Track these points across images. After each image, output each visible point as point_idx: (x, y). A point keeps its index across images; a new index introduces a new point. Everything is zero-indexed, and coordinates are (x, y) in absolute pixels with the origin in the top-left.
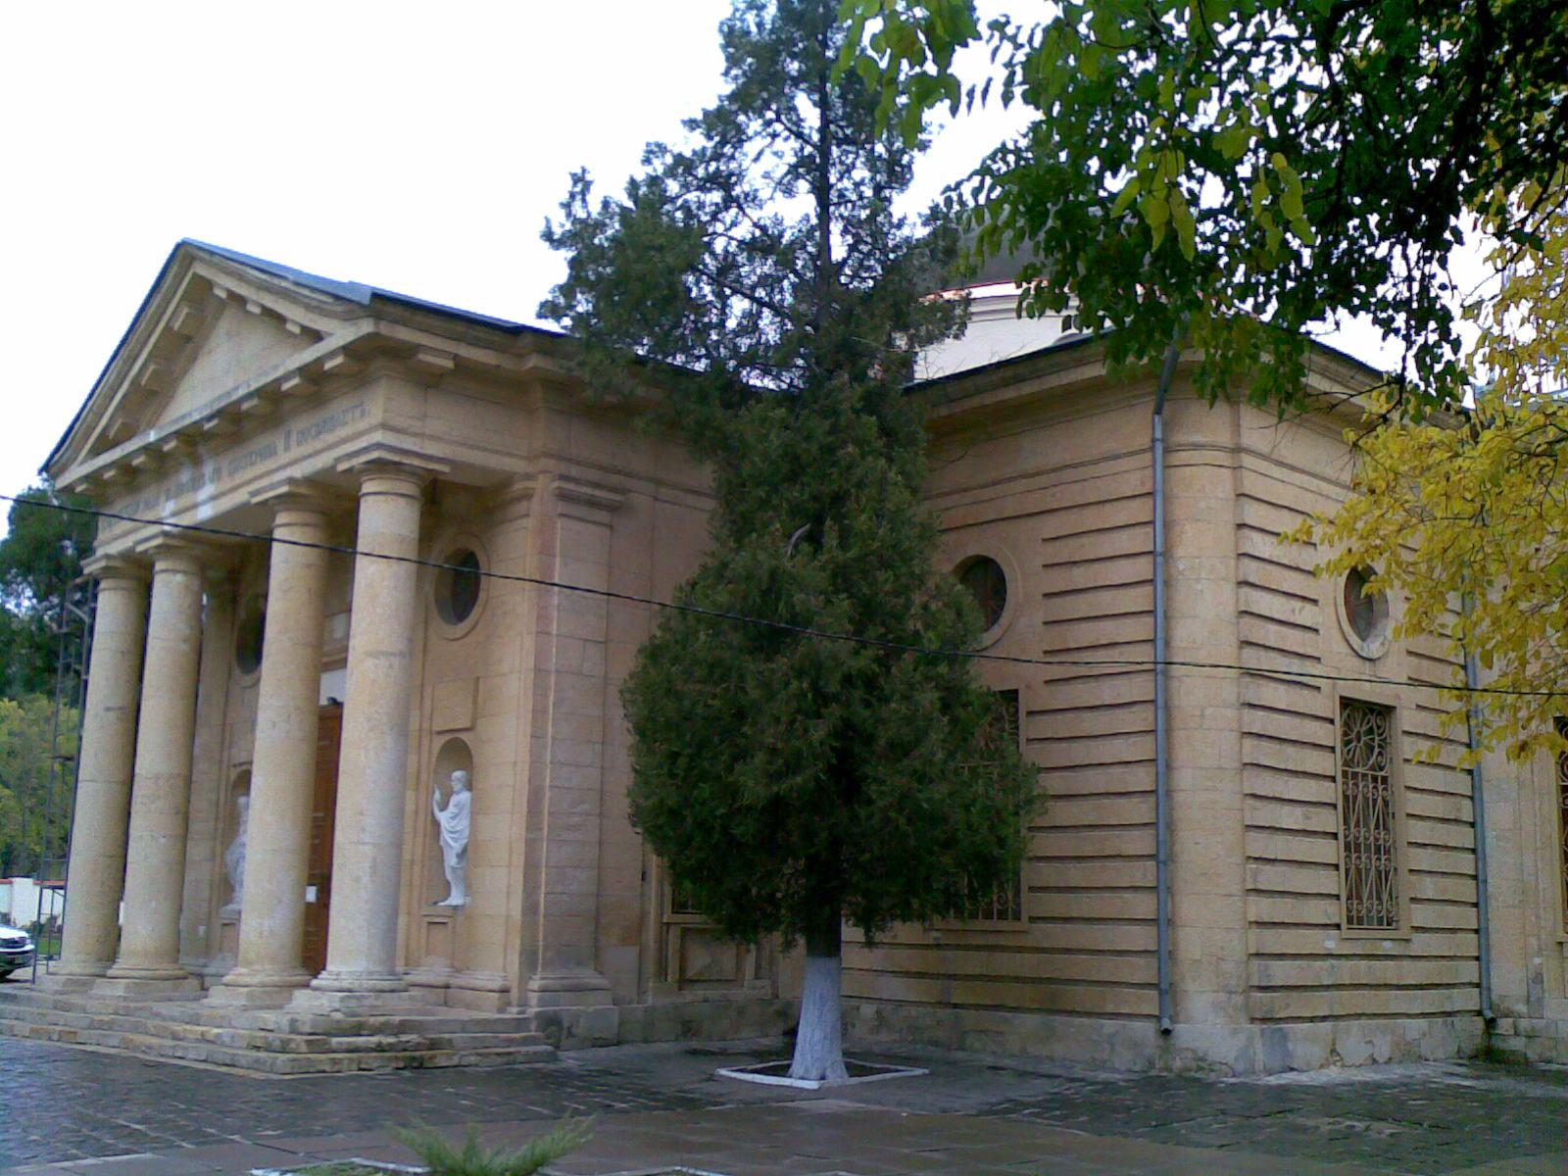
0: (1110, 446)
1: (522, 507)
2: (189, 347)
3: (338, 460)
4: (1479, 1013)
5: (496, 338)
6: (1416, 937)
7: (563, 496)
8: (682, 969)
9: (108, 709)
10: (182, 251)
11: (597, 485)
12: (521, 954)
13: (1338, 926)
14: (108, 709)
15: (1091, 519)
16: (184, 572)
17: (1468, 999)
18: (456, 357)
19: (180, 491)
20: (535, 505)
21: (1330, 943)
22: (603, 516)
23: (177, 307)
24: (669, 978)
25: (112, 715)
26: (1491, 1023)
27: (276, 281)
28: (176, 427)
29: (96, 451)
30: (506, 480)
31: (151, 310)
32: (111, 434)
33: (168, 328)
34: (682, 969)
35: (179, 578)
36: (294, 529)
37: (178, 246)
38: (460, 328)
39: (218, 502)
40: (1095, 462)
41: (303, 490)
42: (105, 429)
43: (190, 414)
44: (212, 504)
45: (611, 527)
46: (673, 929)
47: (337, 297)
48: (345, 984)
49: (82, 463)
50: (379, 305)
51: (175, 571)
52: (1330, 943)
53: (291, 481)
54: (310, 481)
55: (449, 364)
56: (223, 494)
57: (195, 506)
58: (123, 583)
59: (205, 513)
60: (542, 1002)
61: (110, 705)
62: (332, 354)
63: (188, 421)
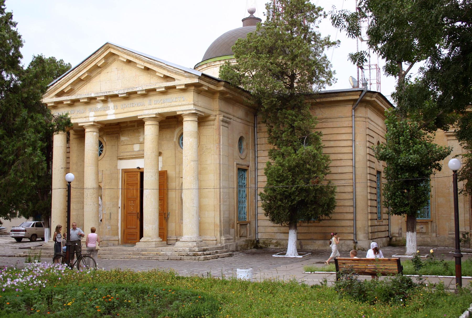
0: (340, 115)
1: (212, 123)
2: (99, 70)
3: (179, 111)
4: (388, 237)
6: (384, 221)
7: (223, 121)
8: (240, 234)
9: (62, 168)
10: (107, 45)
13: (376, 219)
14: (62, 168)
15: (335, 131)
16: (96, 132)
17: (386, 234)
18: (208, 87)
19: (96, 110)
20: (216, 123)
21: (376, 223)
22: (226, 125)
25: (63, 170)
26: (391, 239)
27: (156, 62)
28: (106, 94)
30: (209, 116)
31: (90, 59)
34: (240, 234)
35: (95, 133)
37: (107, 43)
39: (117, 115)
40: (336, 118)
41: (158, 116)
42: (64, 89)
44: (114, 115)
45: (228, 127)
47: (186, 72)
48: (194, 240)
50: (203, 77)
51: (94, 132)
52: (376, 223)
53: (156, 114)
54: (160, 114)
55: (207, 89)
57: (107, 115)
60: (225, 243)
61: (63, 167)
62: (180, 85)
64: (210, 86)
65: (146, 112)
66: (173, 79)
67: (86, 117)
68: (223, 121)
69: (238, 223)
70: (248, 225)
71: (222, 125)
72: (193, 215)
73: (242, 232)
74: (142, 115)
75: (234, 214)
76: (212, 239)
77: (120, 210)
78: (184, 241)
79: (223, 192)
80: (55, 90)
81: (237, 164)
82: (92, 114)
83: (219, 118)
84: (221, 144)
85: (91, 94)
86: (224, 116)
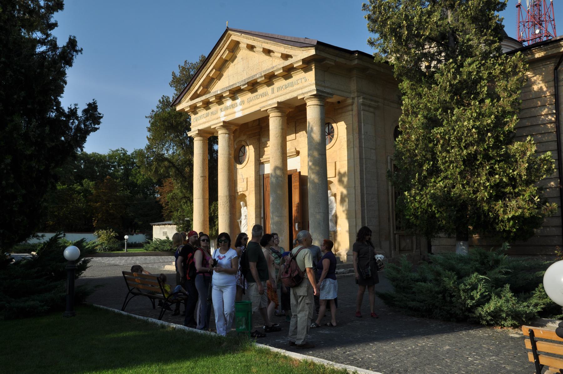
1: (350, 108)
3: (299, 95)
8: (400, 247)
11: (371, 100)
22: (372, 110)
24: (397, 250)
29: (192, 99)
32: (198, 92)
33: (221, 57)
36: (278, 117)
38: (337, 52)
43: (235, 84)
44: (241, 112)
45: (374, 114)
46: (396, 235)
49: (188, 102)
55: (333, 64)
56: (246, 109)
57: (235, 113)
58: (201, 138)
59: (239, 115)
62: (297, 62)
63: (235, 86)
64: (337, 60)
65: (270, 102)
66: (290, 56)
67: (217, 119)
68: (363, 104)
69: (395, 234)
71: (363, 110)
72: (319, 224)
73: (403, 244)
74: (264, 107)
75: (389, 221)
79: (366, 193)
82: (223, 113)
83: (358, 102)
84: (363, 133)
85: (217, 91)
86: (363, 98)
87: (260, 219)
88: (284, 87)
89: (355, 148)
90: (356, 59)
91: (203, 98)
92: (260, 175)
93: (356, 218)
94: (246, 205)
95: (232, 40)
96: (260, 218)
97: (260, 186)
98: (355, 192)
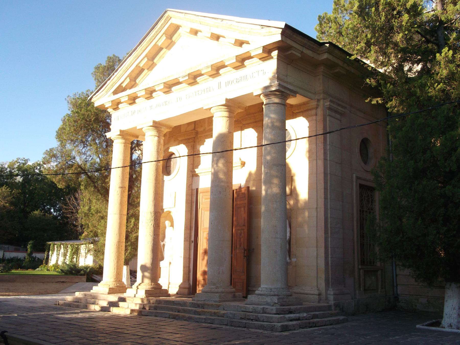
5: (315, 47)
7: (330, 109)
11: (339, 105)
12: (325, 280)
22: (338, 116)
23: (162, 36)
24: (361, 289)
32: (124, 85)
33: (155, 44)
38: (305, 41)
45: (340, 121)
46: (361, 271)
48: (276, 293)
55: (299, 55)
68: (330, 109)
69: (360, 269)
70: (379, 272)
71: (329, 115)
72: (275, 252)
75: (354, 253)
76: (312, 292)
77: (193, 244)
78: (261, 295)
79: (330, 217)
80: (112, 86)
81: (358, 178)
83: (324, 105)
84: (328, 143)
86: (331, 101)
87: (190, 243)
88: (235, 81)
89: (318, 161)
90: (325, 52)
91: (129, 92)
92: (192, 190)
93: (317, 247)
94: (172, 225)
95: (171, 23)
96: (190, 241)
97: (191, 203)
98: (317, 215)
